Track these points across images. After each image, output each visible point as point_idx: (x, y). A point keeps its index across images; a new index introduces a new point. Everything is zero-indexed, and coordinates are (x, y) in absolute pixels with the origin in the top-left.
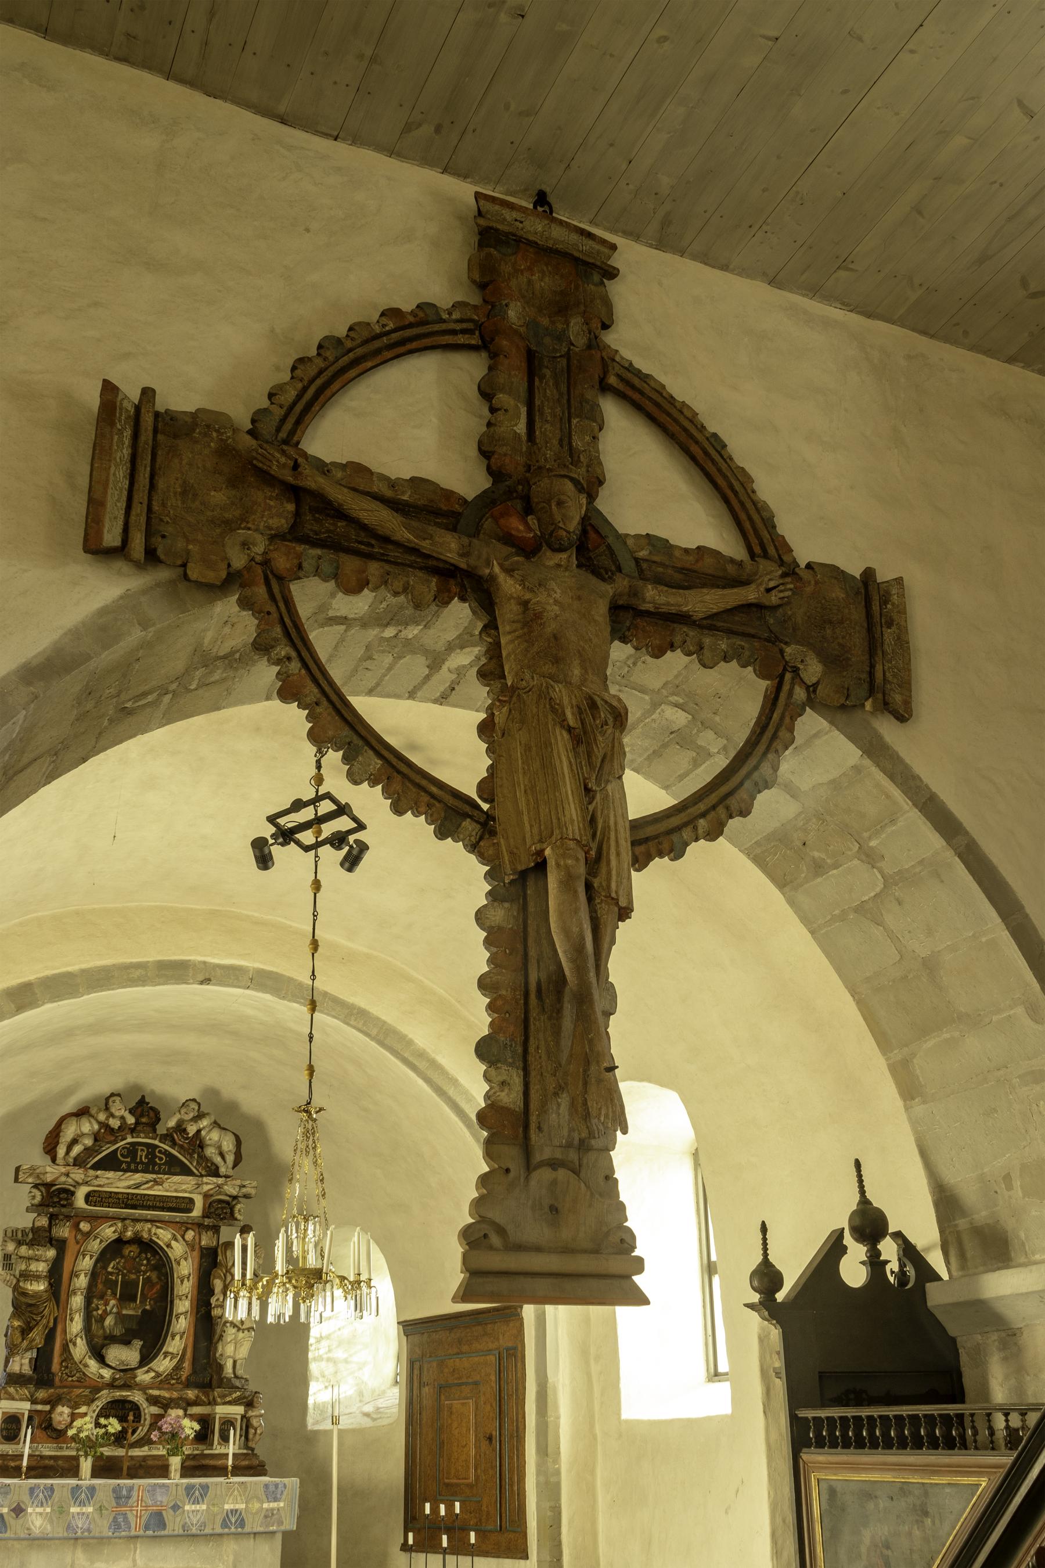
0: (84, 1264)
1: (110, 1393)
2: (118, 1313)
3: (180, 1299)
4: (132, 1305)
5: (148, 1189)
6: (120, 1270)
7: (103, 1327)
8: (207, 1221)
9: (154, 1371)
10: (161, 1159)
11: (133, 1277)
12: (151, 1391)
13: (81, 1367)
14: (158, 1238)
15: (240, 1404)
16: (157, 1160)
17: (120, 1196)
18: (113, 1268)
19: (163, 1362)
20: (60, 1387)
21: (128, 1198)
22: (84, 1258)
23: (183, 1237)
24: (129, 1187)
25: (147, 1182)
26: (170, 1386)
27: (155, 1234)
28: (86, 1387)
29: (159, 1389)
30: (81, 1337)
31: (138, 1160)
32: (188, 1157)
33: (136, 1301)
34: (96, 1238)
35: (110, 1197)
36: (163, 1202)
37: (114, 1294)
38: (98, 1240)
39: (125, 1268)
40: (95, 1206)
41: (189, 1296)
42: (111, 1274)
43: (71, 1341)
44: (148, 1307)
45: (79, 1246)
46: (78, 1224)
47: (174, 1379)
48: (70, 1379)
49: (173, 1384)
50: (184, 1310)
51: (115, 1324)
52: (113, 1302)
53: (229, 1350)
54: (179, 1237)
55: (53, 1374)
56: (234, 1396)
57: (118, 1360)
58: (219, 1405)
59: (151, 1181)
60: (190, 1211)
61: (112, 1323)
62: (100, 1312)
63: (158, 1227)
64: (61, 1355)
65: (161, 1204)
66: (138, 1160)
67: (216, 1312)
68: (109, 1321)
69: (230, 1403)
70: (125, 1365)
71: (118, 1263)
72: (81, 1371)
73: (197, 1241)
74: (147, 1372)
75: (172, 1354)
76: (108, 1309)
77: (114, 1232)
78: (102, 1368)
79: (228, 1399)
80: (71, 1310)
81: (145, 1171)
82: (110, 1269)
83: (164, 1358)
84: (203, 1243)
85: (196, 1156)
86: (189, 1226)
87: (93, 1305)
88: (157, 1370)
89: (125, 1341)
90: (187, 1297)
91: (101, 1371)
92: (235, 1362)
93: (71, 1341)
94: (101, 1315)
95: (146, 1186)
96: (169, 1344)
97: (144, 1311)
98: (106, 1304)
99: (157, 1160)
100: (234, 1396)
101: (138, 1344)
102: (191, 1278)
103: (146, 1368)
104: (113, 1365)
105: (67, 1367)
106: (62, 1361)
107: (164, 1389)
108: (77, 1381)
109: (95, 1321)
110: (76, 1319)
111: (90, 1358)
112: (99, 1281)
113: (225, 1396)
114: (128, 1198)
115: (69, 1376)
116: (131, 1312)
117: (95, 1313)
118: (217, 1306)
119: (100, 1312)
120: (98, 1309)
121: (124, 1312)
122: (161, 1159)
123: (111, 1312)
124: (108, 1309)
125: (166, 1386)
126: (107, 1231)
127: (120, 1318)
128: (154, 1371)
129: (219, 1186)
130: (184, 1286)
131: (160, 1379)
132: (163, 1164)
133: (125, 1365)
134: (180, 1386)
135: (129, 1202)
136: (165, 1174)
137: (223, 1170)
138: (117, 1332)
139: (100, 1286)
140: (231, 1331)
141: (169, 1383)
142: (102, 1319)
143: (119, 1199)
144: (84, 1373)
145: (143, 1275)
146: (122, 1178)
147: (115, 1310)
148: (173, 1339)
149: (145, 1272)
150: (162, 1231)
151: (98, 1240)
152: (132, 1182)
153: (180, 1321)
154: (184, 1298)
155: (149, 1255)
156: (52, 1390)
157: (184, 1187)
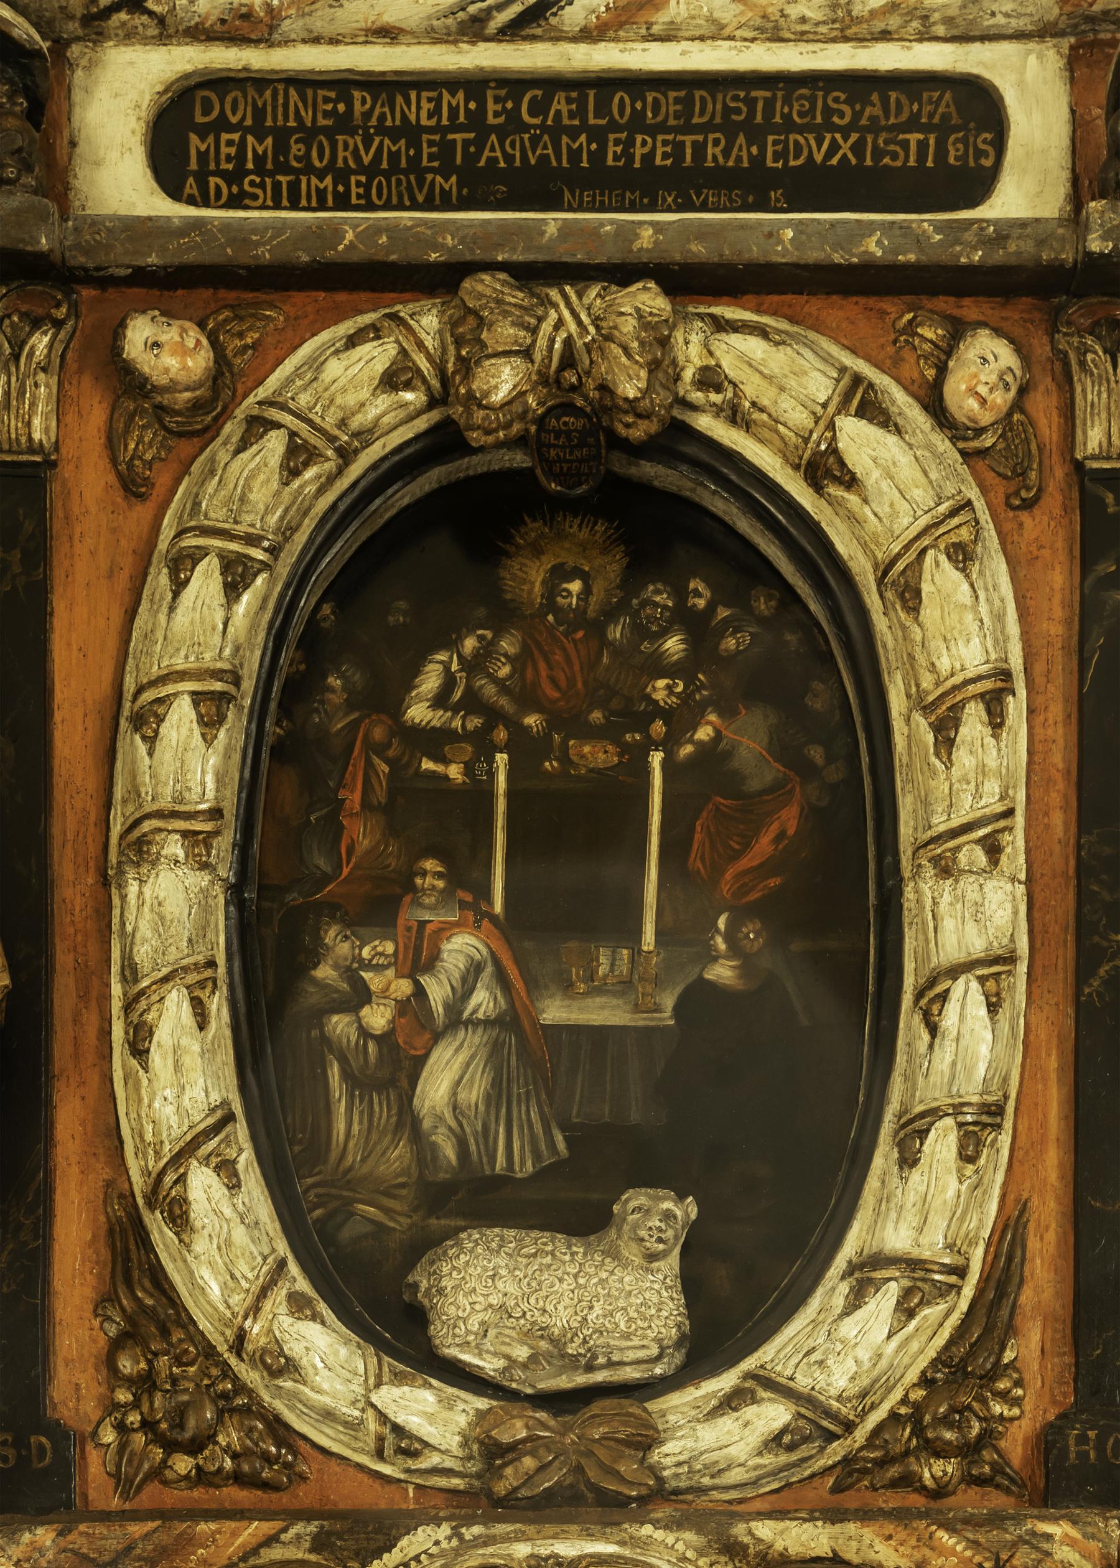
0: (183, 617)
1: (466, 1546)
3: (946, 870)
9: (786, 1392)
12: (765, 1530)
13: (251, 1376)
14: (734, 415)
17: (420, 110)
19: (849, 1328)
20: (105, 1517)
21: (476, 120)
22: (179, 586)
26: (917, 1501)
27: (710, 379)
28: (306, 1515)
29: (834, 1516)
30: (226, 1169)
34: (258, 427)
35: (344, 124)
36: (756, 135)
38: (275, 444)
39: (528, 700)
40: (236, 202)
41: (1015, 843)
43: (152, 1201)
45: (143, 512)
46: (118, 331)
47: (940, 1451)
48: (183, 1464)
49: (940, 1492)
50: (977, 945)
54: (900, 399)
55: (61, 1435)
57: (526, 1336)
63: (721, 326)
64: (105, 1301)
65: (743, 151)
70: (573, 1363)
72: (254, 1409)
73: (1048, 427)
74: (732, 1402)
75: (913, 1264)
77: (391, 381)
78: (399, 1379)
80: (131, 972)
83: (855, 1302)
84: (1093, 438)
86: (970, 309)
88: (803, 1382)
90: (993, 849)
91: (387, 1397)
93: (152, 1201)
96: (884, 1199)
102: (1016, 707)
103: (726, 1381)
104: (490, 1366)
105: (145, 1383)
106: (116, 1345)
107: (865, 1515)
108: (238, 1478)
110: (163, 1035)
111: (298, 1305)
114: (476, 120)
115: (171, 1447)
125: (889, 1500)
126: (334, 368)
128: (786, 1392)
130: (963, 759)
131: (837, 1451)
133: (573, 1363)
134: (997, 1500)
135: (492, 151)
141: (908, 1481)
143: (411, 132)
144: (278, 1428)
148: (908, 1160)
150: (754, 346)
151: (275, 444)
153: (950, 1019)
154: (972, 855)
156: (44, 1536)
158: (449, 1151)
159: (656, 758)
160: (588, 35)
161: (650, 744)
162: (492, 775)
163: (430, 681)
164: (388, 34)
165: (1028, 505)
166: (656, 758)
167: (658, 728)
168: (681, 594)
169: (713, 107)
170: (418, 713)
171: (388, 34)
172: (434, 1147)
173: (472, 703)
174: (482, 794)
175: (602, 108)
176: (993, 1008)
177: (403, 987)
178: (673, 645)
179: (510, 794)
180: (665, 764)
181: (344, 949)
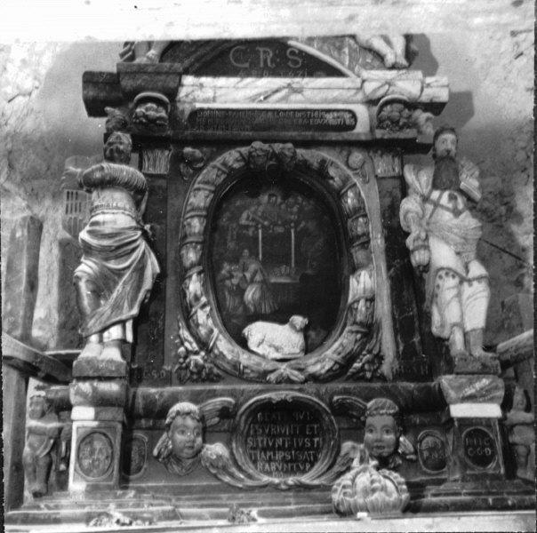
2: (264, 282)
4: (283, 268)
5: (279, 101)
6: (258, 223)
7: (242, 302)
8: (379, 134)
10: (296, 62)
11: (280, 230)
15: (492, 400)
16: (290, 64)
18: (248, 219)
23: (347, 164)
24: (253, 99)
25: (277, 91)
31: (262, 65)
32: (336, 54)
33: (288, 263)
37: (254, 254)
42: (247, 227)
44: (309, 272)
51: (263, 297)
52: (253, 267)
53: (452, 314)
56: (478, 385)
58: (455, 402)
59: (284, 88)
60: (352, 127)
61: (257, 296)
62: (235, 281)
66: (262, 65)
67: (418, 258)
68: (251, 294)
69: (471, 398)
71: (255, 213)
76: (248, 275)
79: (469, 391)
81: (274, 73)
82: (243, 221)
85: (346, 50)
87: (223, 272)
89: (280, 317)
92: (465, 334)
94: (238, 286)
95: (278, 95)
97: (304, 278)
98: (244, 269)
99: (290, 64)
100: (478, 385)
101: (299, 320)
109: (229, 292)
112: (229, 238)
113: (460, 388)
116: (282, 280)
117: (228, 282)
118: (417, 249)
119: (235, 281)
120: (231, 277)
121: (273, 280)
122: (296, 62)
123: (252, 281)
124: (248, 275)
127: (268, 289)
129: (389, 83)
132: (299, 69)
136: (303, 76)
137: (390, 59)
138: (266, 309)
139: (231, 245)
140: (449, 283)
142: (240, 291)
145: (296, 227)
146: (241, 85)
147: (258, 278)
149: (297, 223)
152: (255, 92)
155: (300, 199)
157: (336, 93)
158: (252, 308)
159: (292, 231)
160: (274, 103)
161: (291, 228)
162: (258, 234)
163: (244, 215)
164: (235, 102)
165: (368, 182)
166: (292, 231)
167: (292, 225)
168: (296, 199)
169: (300, 114)
170: (243, 221)
171: (235, 102)
172: (249, 308)
173: (253, 220)
174: (256, 238)
175: (278, 114)
176: (370, 277)
177: (241, 275)
178: (295, 209)
179: (263, 238)
180: (295, 232)
181: (228, 268)
